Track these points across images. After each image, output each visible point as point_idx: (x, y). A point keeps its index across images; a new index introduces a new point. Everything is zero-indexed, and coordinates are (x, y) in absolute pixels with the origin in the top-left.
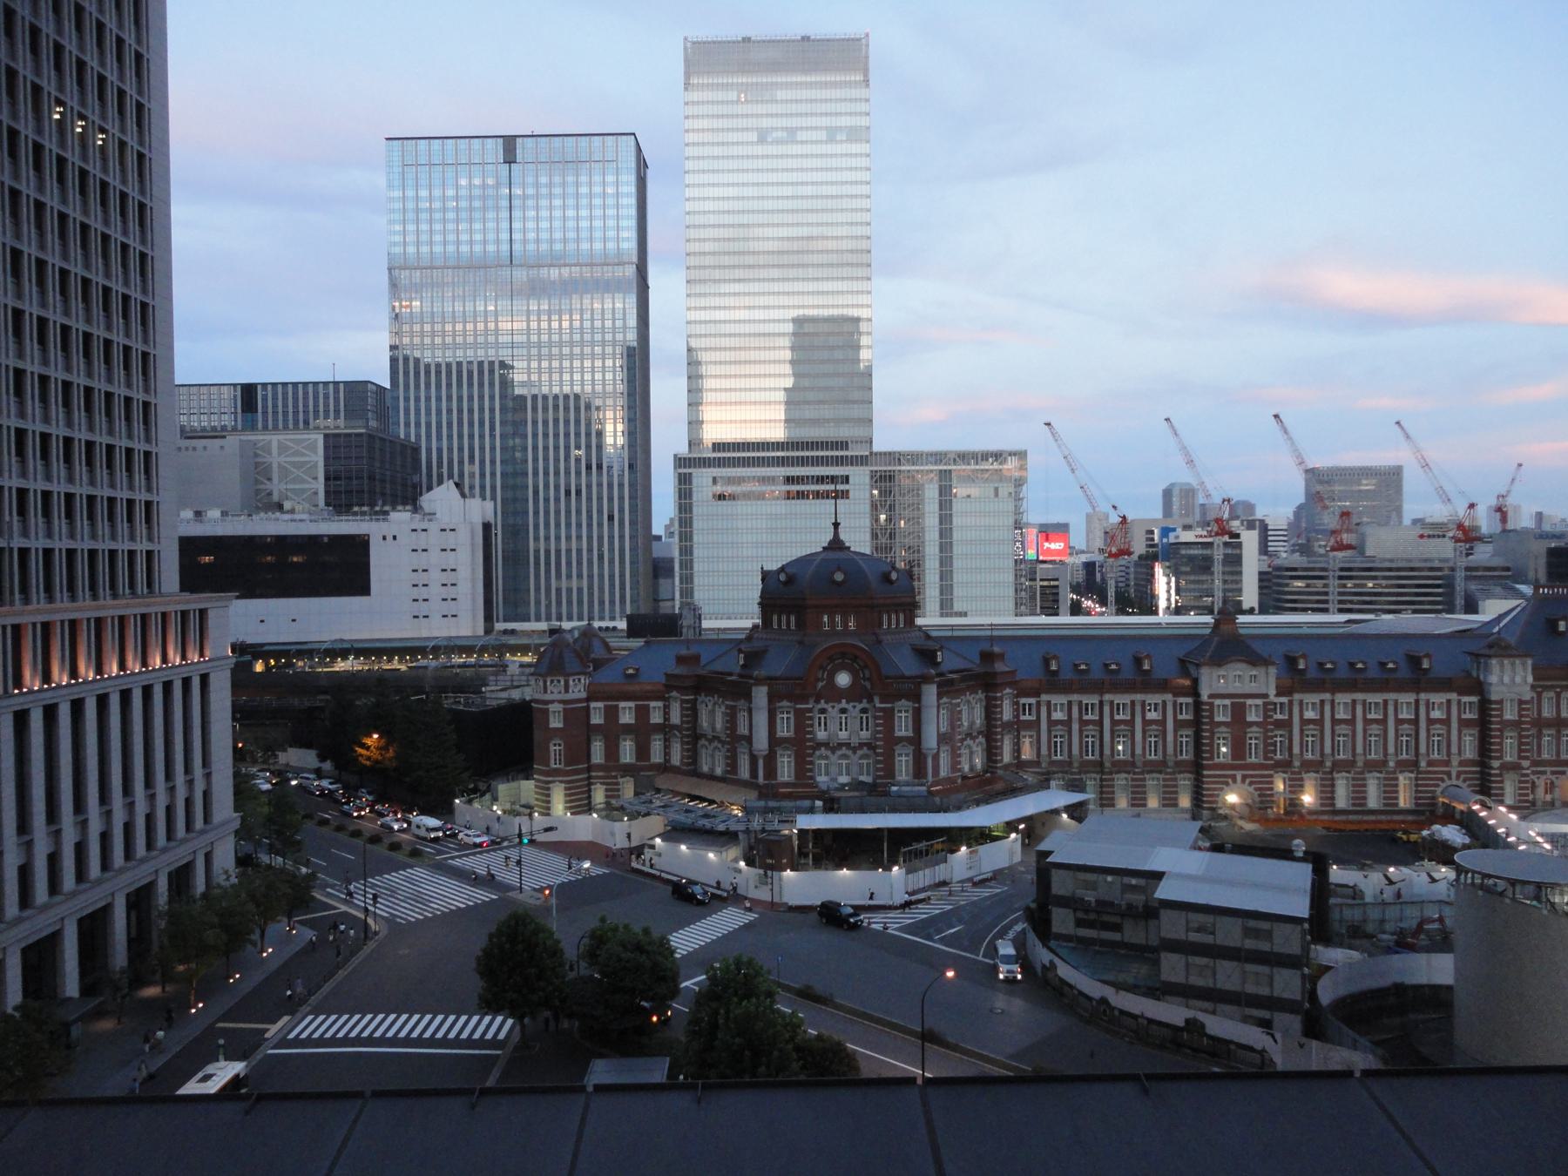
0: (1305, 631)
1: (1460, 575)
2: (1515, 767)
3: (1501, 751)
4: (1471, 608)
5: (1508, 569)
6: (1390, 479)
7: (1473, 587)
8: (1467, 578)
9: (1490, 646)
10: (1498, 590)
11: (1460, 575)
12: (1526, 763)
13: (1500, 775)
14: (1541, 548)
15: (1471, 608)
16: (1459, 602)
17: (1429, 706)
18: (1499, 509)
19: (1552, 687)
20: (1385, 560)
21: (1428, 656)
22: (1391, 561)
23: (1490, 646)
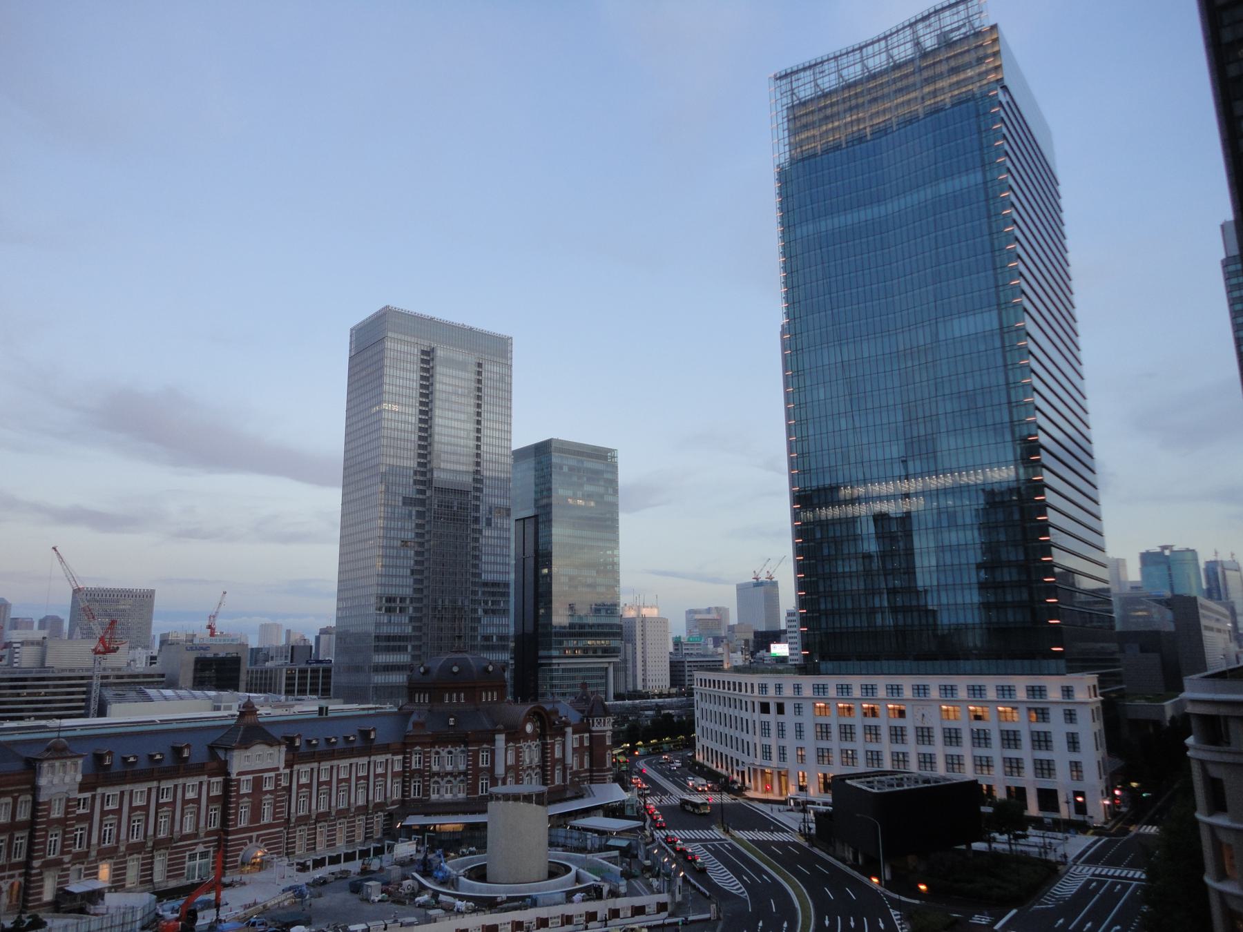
0: (78, 733)
1: (96, 682)
2: (58, 863)
3: (44, 850)
4: (102, 712)
5: (163, 676)
6: (146, 598)
7: (108, 694)
8: (102, 685)
9: (48, 750)
10: (133, 694)
11: (96, 682)
12: (67, 858)
13: (41, 874)
14: (191, 657)
15: (102, 712)
16: (94, 706)
17: (105, 800)
18: (209, 627)
19: (12, 792)
20: (63, 670)
21: (188, 746)
22: (71, 670)
23: (48, 750)
